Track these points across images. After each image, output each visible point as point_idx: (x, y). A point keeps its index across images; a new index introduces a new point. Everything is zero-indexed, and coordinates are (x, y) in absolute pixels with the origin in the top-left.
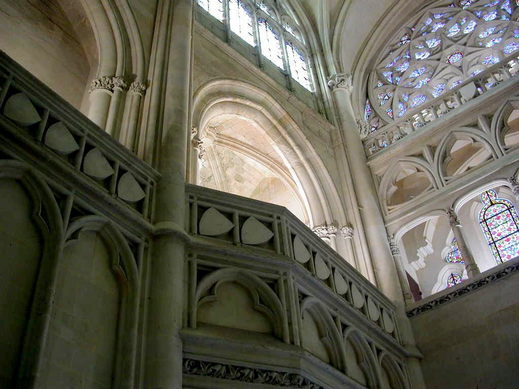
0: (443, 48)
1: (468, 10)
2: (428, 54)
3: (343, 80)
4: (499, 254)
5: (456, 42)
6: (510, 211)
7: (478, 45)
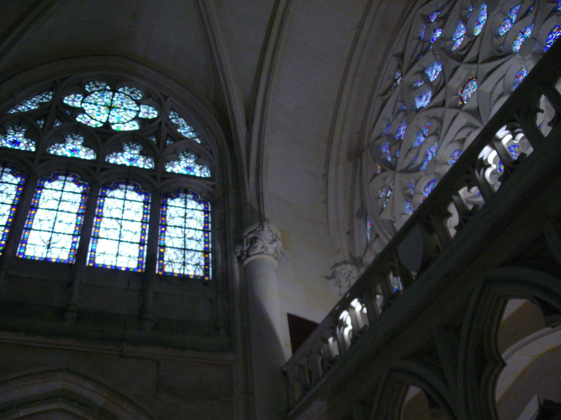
0: (447, 79)
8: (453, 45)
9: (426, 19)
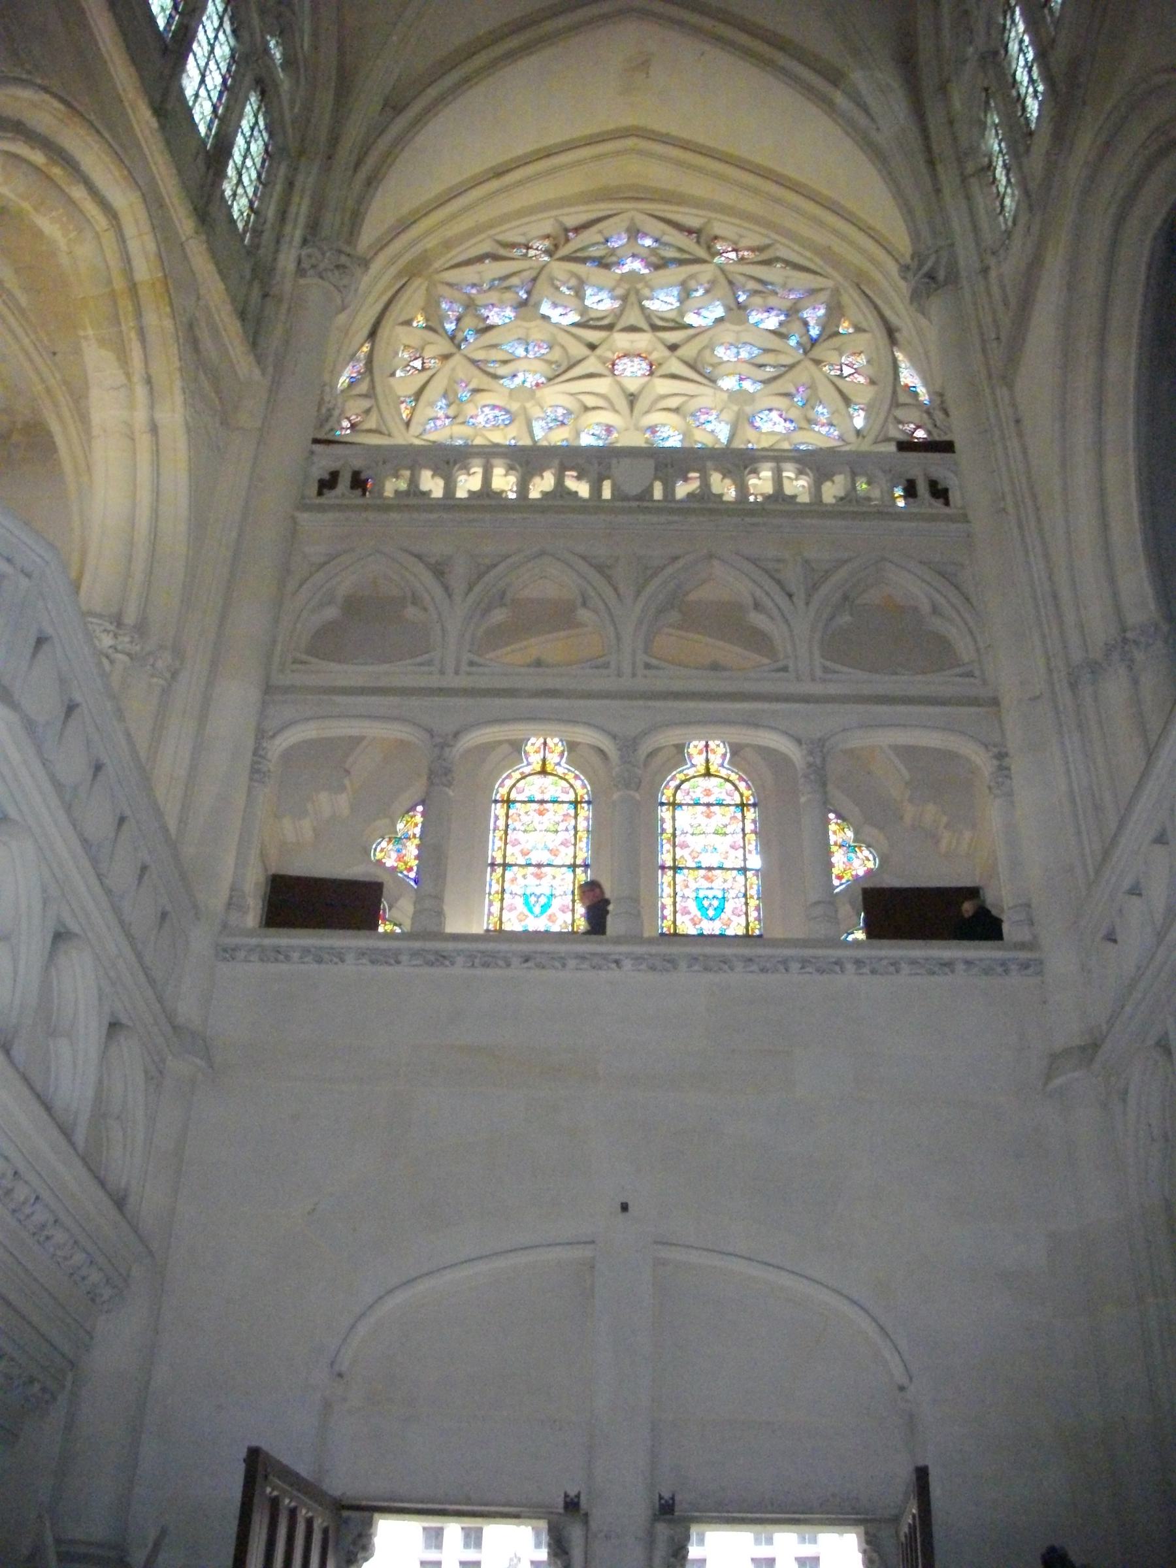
0: (619, 327)
1: (723, 271)
2: (574, 317)
3: (344, 267)
4: (502, 900)
5: (655, 328)
6: (576, 808)
7: (703, 371)
8: (648, 299)
9: (634, 233)
